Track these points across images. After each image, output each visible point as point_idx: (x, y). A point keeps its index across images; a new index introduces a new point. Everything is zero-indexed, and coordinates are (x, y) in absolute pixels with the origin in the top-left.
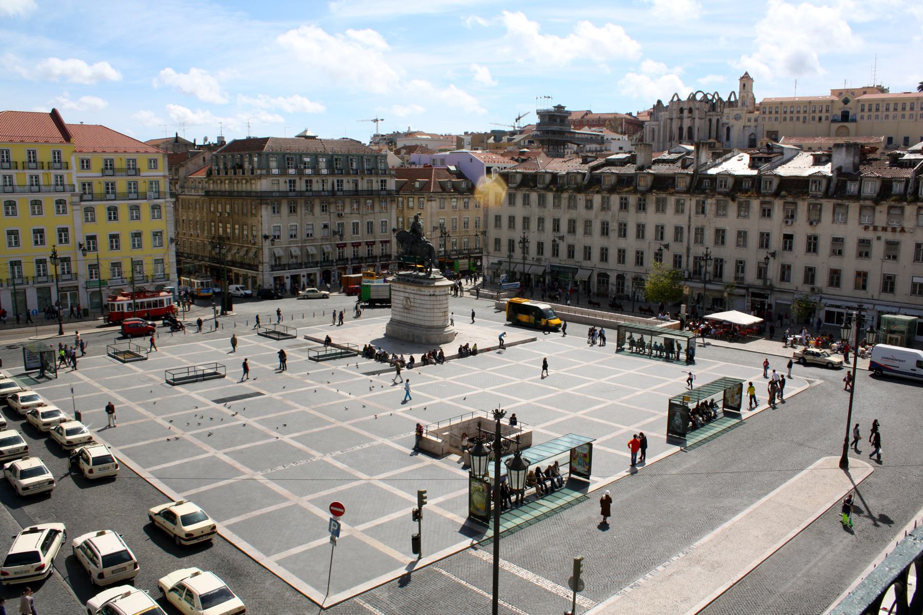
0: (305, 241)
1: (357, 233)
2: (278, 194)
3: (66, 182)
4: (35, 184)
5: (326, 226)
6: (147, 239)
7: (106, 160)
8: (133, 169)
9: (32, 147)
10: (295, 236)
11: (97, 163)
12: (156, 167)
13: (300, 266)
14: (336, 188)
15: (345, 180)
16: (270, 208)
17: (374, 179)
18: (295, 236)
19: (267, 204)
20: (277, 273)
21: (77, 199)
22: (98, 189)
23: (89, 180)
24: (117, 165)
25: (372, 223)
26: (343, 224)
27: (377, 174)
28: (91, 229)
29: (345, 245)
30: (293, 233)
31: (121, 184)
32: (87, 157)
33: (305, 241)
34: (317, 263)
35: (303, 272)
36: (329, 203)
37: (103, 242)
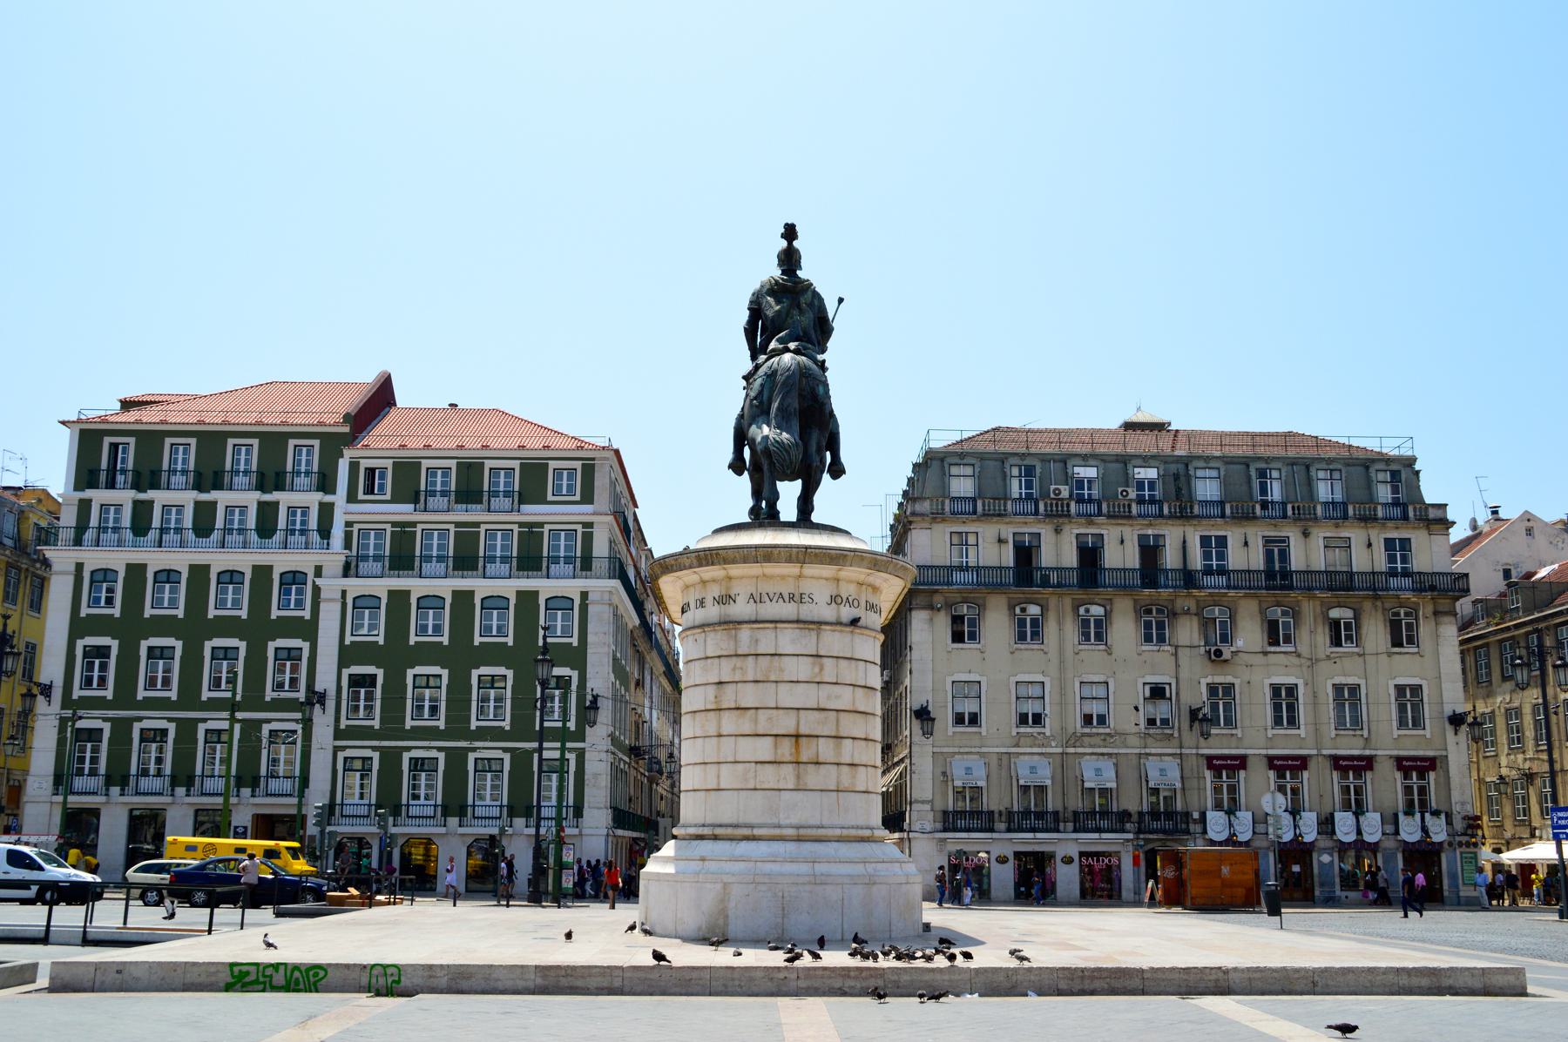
0: (1076, 740)
1: (1293, 722)
2: (969, 577)
5: (1157, 692)
10: (1038, 719)
13: (1050, 821)
15: (1234, 536)
16: (943, 623)
17: (1356, 535)
18: (1038, 719)
19: (931, 607)
20: (960, 841)
25: (1354, 690)
26: (1229, 689)
27: (1367, 519)
29: (1241, 762)
30: (1031, 708)
33: (1076, 740)
34: (1124, 816)
35: (1066, 844)
36: (1174, 615)
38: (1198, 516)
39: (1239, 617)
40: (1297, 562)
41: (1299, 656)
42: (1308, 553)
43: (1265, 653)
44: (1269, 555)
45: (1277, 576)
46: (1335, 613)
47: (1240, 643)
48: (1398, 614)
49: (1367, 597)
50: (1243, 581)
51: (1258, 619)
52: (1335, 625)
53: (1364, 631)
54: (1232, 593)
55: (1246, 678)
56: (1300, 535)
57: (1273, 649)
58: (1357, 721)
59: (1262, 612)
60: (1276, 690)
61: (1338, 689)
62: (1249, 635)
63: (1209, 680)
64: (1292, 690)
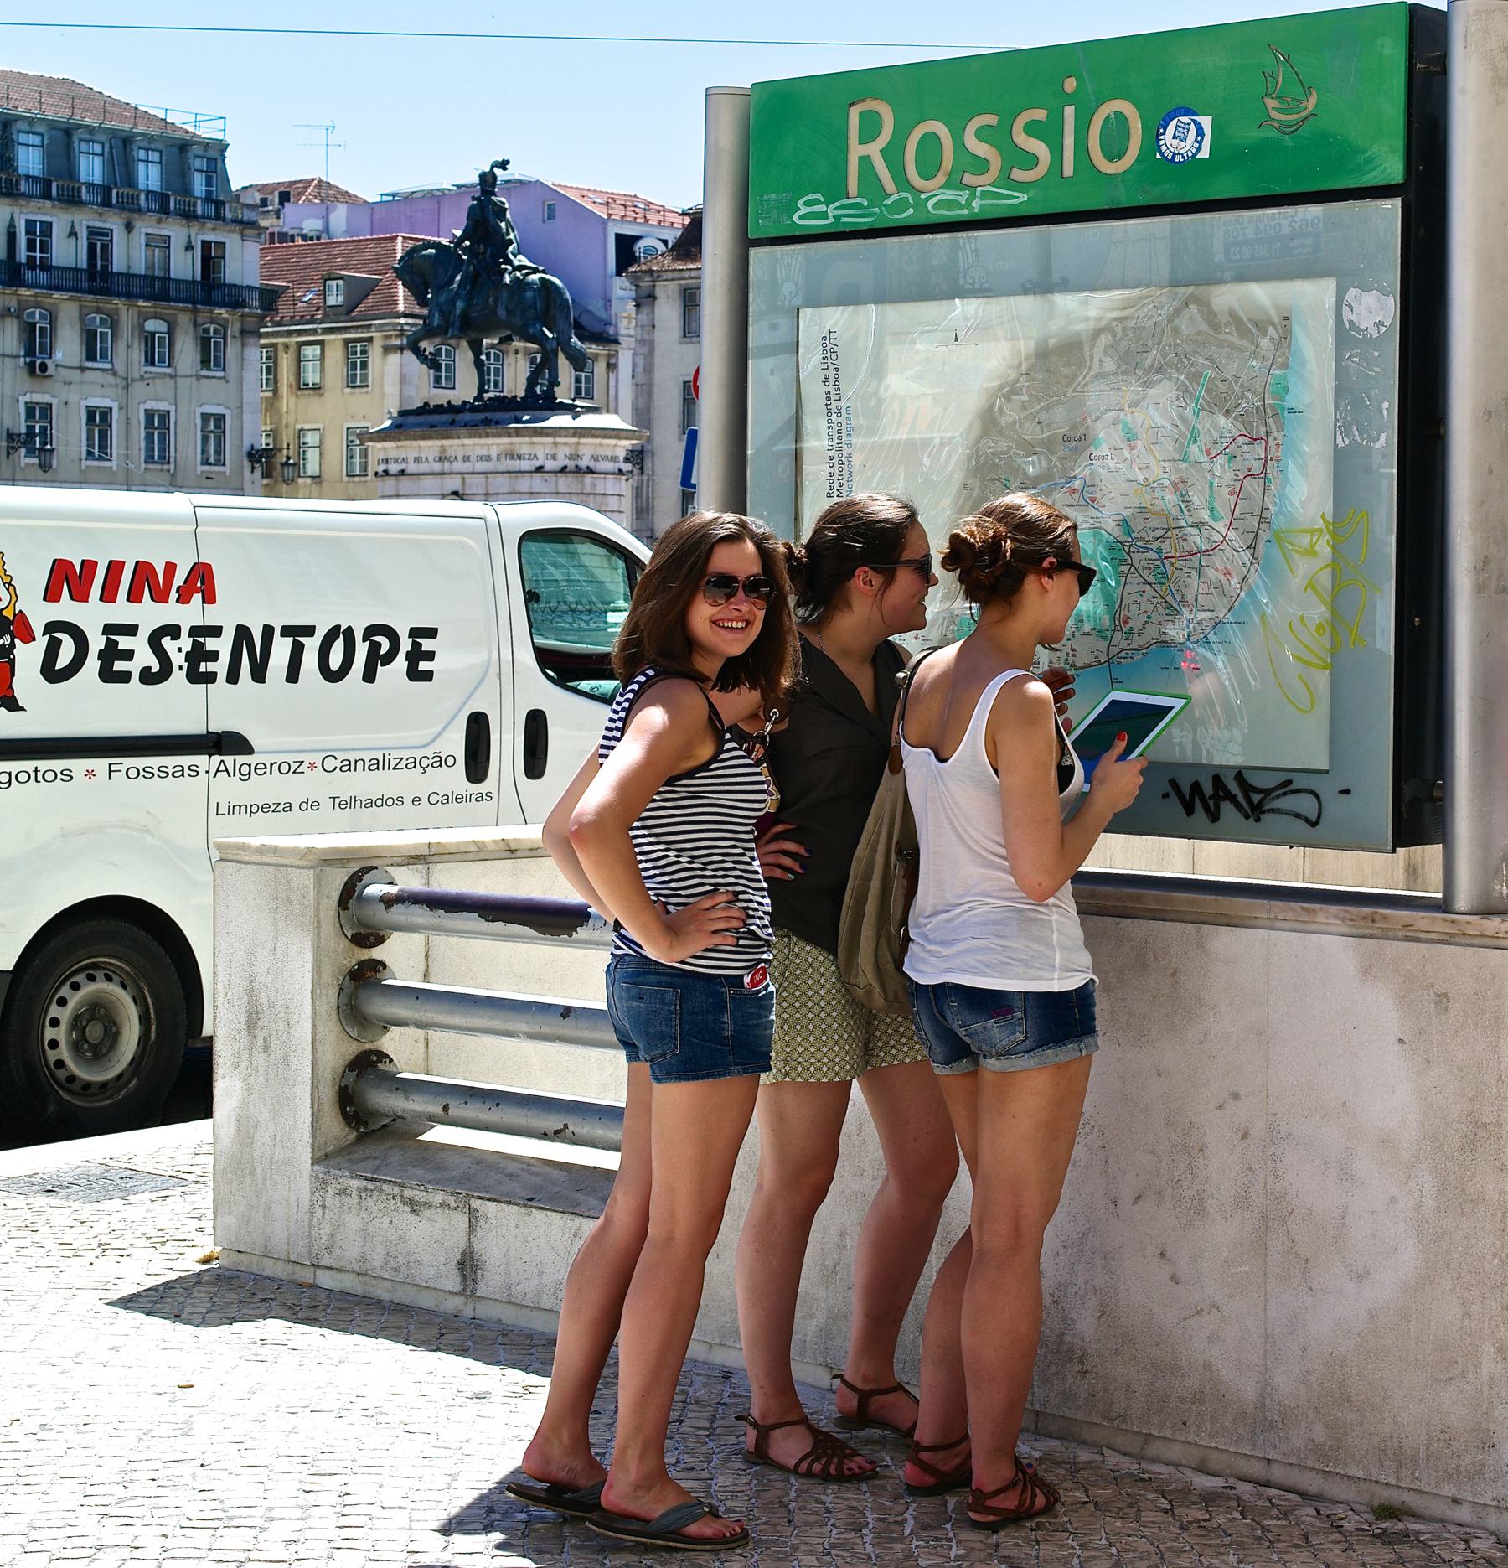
14: (22, 254)
25: (164, 416)
26: (46, 409)
38: (23, 195)
39: (59, 325)
40: (118, 265)
41: (115, 374)
42: (129, 253)
43: (83, 369)
44: (91, 248)
45: (97, 277)
46: (150, 325)
47: (58, 356)
48: (207, 331)
49: (184, 310)
50: (64, 280)
51: (78, 327)
52: (149, 339)
53: (178, 347)
54: (56, 295)
55: (63, 398)
56: (122, 228)
57: (90, 364)
58: (164, 459)
59: (82, 318)
60: (91, 413)
61: (149, 415)
62: (67, 347)
63: (27, 398)
64: (106, 414)
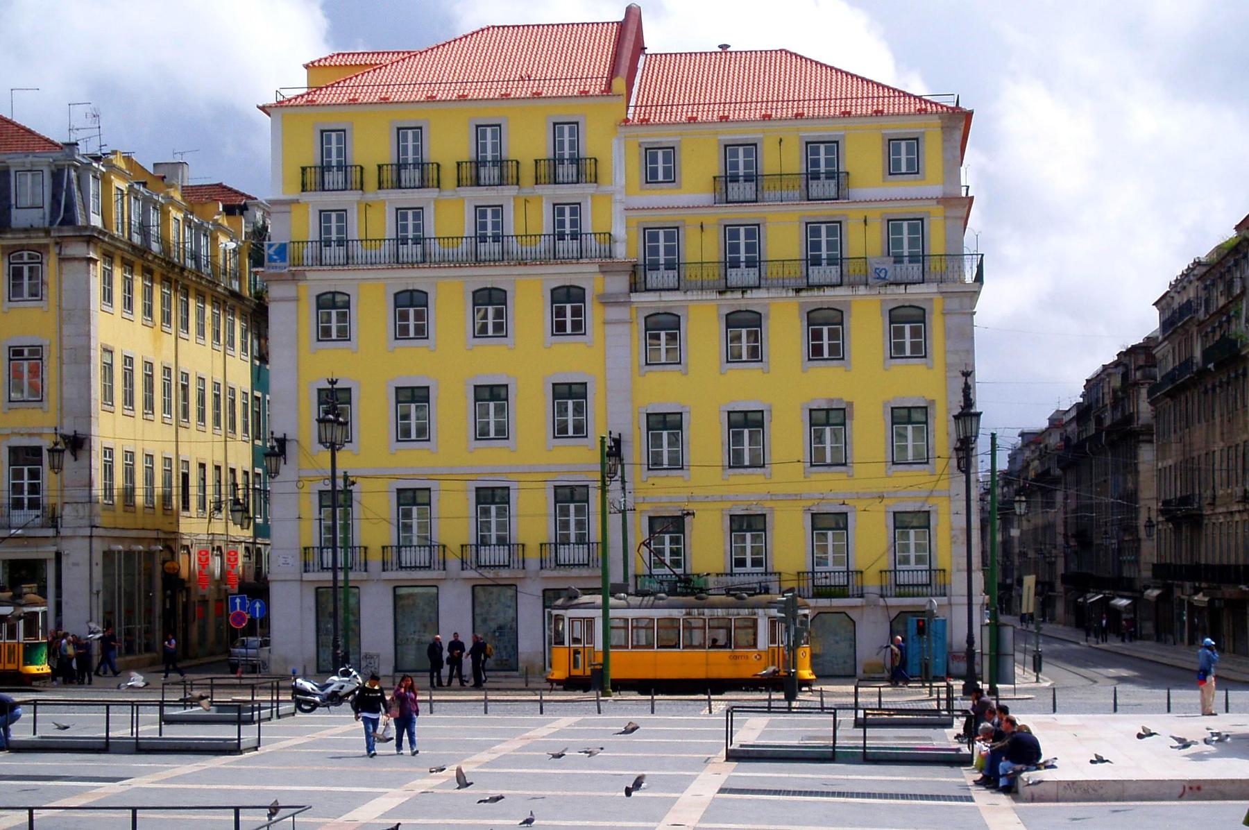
3: (588, 225)
4: (488, 227)
6: (869, 434)
7: (729, 149)
8: (823, 169)
9: (488, 115)
11: (700, 165)
12: (914, 169)
21: (620, 283)
22: (702, 248)
23: (668, 218)
24: (769, 163)
28: (663, 390)
31: (783, 238)
32: (666, 138)
37: (705, 439)
